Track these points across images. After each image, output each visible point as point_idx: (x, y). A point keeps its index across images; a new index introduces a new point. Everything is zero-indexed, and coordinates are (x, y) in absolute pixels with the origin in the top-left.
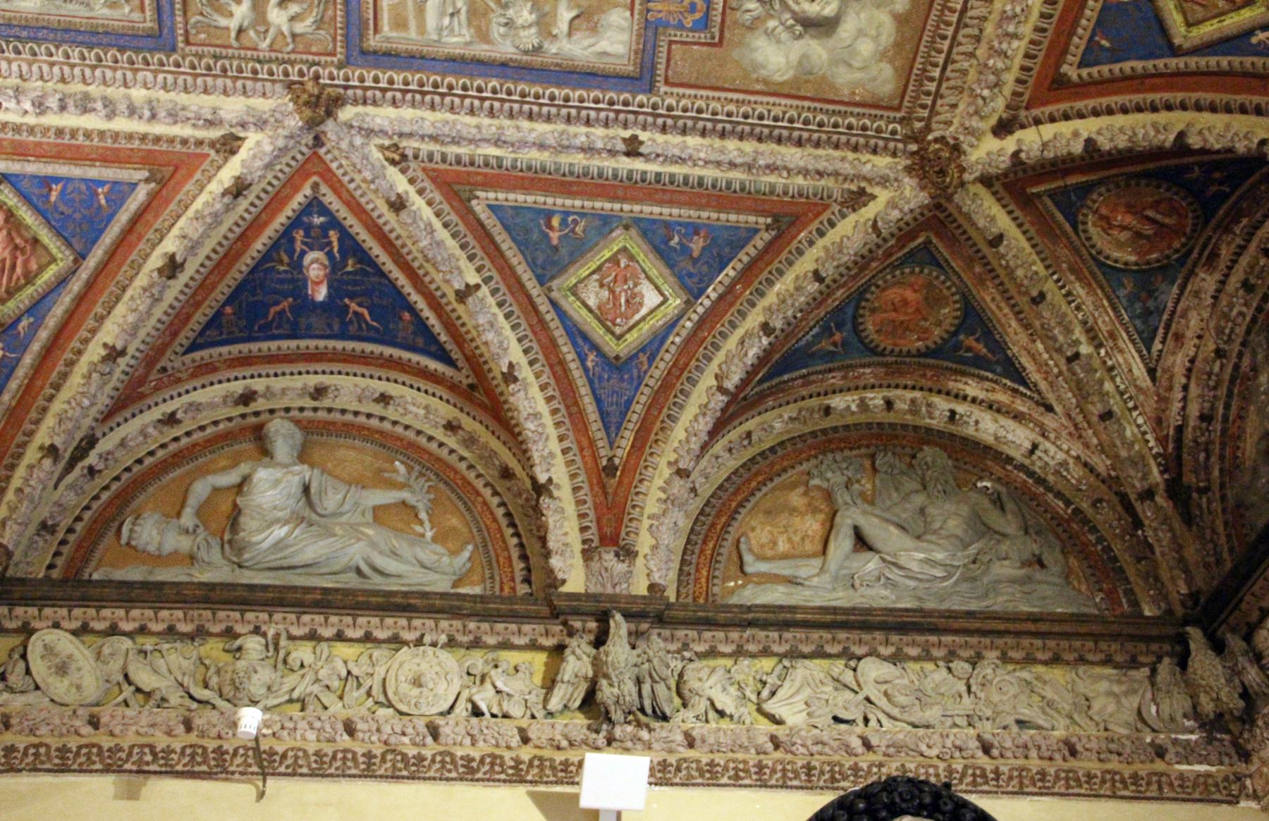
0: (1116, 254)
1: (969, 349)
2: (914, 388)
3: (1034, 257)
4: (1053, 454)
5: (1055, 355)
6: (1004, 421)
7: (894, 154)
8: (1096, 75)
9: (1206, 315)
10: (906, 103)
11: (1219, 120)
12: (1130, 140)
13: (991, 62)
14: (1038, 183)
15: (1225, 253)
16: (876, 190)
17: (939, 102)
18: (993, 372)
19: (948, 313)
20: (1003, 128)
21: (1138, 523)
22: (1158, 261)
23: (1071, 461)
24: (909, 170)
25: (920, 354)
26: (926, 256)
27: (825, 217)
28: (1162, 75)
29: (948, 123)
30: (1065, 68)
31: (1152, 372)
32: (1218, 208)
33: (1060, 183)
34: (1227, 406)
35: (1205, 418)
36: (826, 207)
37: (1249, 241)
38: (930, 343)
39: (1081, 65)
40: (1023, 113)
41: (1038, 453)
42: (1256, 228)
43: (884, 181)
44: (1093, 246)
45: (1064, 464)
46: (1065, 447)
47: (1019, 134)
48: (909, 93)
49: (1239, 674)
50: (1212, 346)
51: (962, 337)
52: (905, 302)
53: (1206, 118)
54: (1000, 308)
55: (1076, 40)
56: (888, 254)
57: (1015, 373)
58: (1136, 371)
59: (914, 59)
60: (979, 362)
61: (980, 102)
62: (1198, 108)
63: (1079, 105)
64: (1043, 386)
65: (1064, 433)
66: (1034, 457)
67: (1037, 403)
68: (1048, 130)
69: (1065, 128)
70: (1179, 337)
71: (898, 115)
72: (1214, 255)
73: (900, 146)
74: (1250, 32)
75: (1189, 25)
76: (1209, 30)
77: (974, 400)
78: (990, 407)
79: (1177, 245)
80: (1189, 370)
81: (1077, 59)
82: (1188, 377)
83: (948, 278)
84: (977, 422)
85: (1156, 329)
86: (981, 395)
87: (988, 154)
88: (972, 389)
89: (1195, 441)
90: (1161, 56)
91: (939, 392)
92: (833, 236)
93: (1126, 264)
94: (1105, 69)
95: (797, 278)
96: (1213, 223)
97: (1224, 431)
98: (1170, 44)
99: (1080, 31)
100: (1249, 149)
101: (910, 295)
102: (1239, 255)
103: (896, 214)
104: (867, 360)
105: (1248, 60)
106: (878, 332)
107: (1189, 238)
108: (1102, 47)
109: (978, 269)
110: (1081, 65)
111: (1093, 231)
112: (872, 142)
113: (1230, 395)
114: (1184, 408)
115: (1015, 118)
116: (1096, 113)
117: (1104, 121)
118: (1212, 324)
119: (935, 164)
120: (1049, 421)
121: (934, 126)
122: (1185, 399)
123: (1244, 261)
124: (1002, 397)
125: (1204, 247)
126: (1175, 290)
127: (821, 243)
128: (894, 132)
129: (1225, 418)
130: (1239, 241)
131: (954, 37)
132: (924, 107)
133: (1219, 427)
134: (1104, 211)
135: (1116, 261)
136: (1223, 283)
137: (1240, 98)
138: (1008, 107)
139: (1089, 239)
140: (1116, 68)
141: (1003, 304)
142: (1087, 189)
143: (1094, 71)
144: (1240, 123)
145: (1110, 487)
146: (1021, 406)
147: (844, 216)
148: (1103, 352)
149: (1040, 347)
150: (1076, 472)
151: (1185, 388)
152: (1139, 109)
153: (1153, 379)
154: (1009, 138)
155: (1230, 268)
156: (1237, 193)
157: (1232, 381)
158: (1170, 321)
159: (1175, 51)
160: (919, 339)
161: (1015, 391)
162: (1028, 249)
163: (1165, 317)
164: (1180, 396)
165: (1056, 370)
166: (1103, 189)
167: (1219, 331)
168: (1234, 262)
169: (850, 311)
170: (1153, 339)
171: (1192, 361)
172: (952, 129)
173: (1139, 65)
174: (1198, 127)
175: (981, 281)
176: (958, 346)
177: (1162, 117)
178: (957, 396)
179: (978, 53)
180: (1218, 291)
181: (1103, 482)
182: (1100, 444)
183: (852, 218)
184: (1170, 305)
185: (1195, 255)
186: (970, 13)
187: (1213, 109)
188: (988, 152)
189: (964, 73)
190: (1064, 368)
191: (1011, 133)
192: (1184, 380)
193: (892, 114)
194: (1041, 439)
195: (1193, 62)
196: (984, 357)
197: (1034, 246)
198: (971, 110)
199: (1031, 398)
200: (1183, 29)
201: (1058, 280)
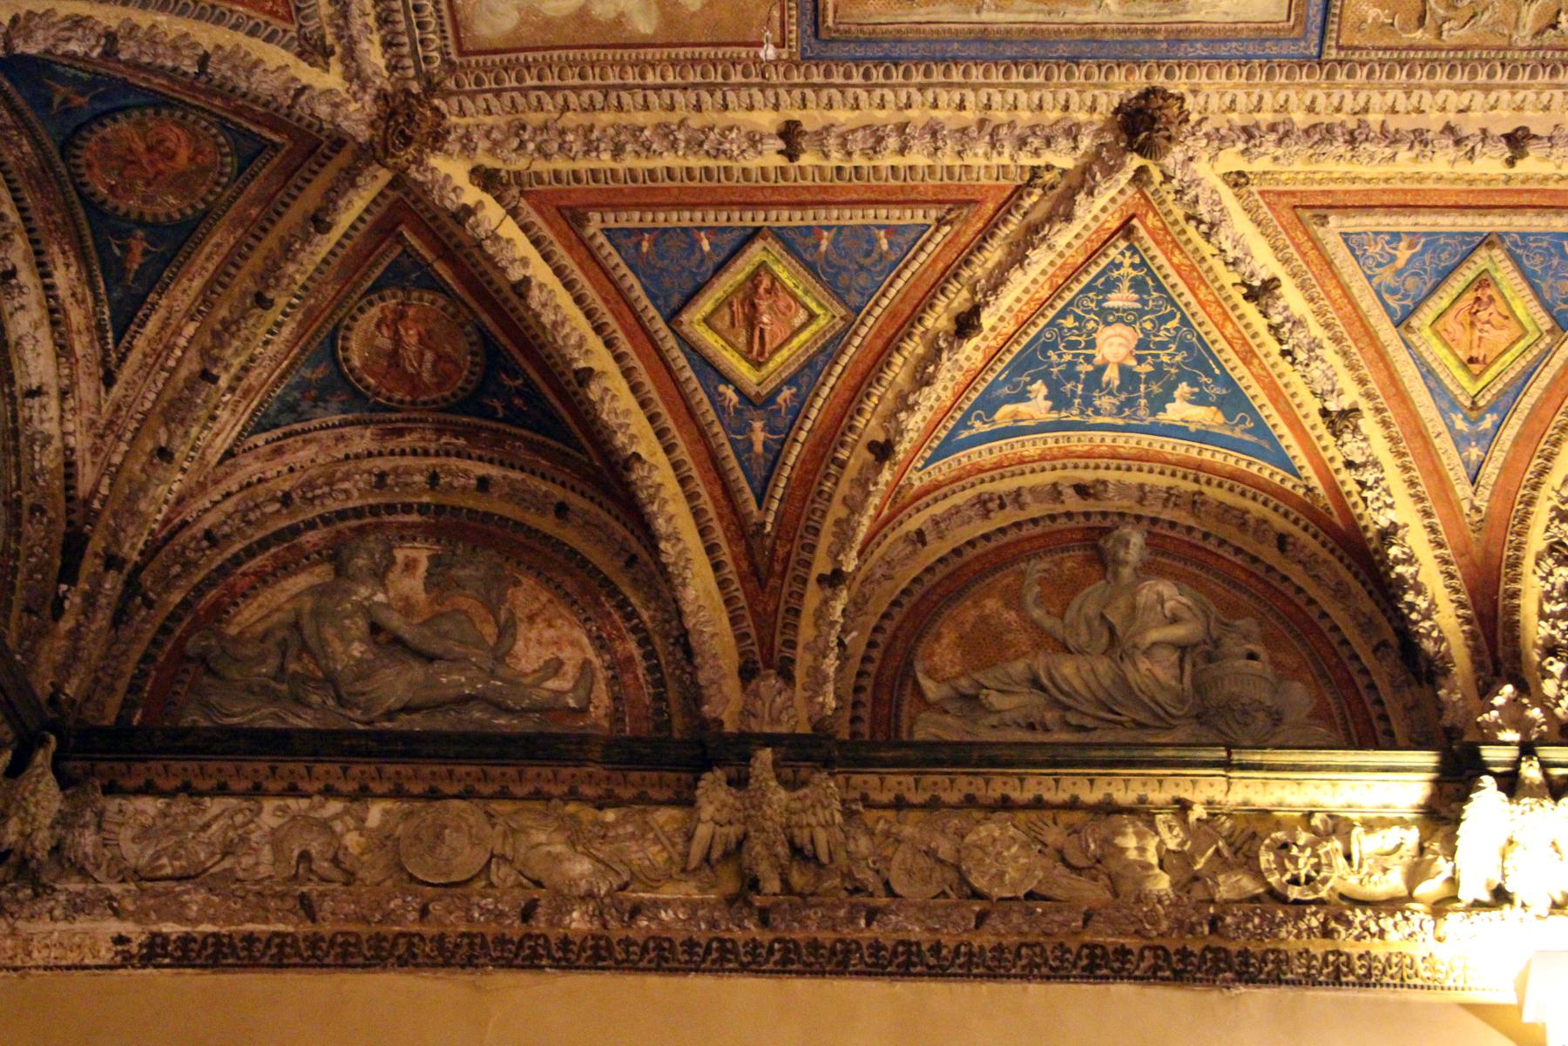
0: (353, 345)
1: (126, 249)
2: (21, 210)
3: (311, 268)
4: (46, 417)
5: (193, 353)
6: (44, 333)
7: (392, 68)
8: (605, 252)
9: (320, 461)
10: (473, 60)
11: (627, 401)
12: (555, 324)
13: (570, 137)
14: (416, 233)
15: (408, 440)
16: (336, 67)
17: (489, 96)
18: (109, 290)
19: (170, 204)
20: (486, 179)
21: (69, 573)
22: (367, 388)
23: (57, 443)
24: (382, 96)
25: (88, 201)
26: (250, 152)
27: (277, 24)
28: (638, 319)
29: (462, 113)
30: (595, 217)
31: (229, 454)
32: (468, 414)
33: (429, 257)
34: (250, 552)
35: (208, 535)
36: (288, 18)
37: (437, 454)
38: (112, 202)
39: (608, 232)
40: (515, 191)
41: (36, 402)
42: (458, 455)
43: (355, 74)
44: (354, 319)
45: (48, 440)
46: (70, 427)
47: (488, 199)
48: (489, 59)
49: (68, 826)
50: (286, 487)
51: (140, 233)
52: (171, 156)
53: (620, 386)
54: (208, 259)
55: (636, 215)
56: (238, 111)
57: (126, 316)
58: (219, 440)
59: (537, 49)
60: (113, 270)
61: (515, 143)
62: (627, 373)
63: (558, 249)
64: (134, 358)
65: (86, 414)
66: (30, 402)
67: (104, 362)
68: (510, 229)
69: (523, 246)
70: (279, 451)
71: (454, 57)
72: (400, 433)
73: (411, 72)
74: (727, 380)
75: (706, 320)
76: (711, 341)
77: (49, 288)
78: (52, 311)
79: (398, 396)
80: (249, 485)
81: (611, 224)
82: (241, 489)
83: (225, 187)
84: (22, 307)
85: (277, 426)
86: (63, 291)
87: (448, 177)
88: (64, 277)
89: (184, 548)
90: (658, 308)
91: (33, 242)
92: (256, 47)
93: (347, 360)
94: (616, 259)
95: (186, 35)
96: (442, 416)
97: (223, 571)
98: (678, 311)
99: (649, 216)
100: (624, 448)
101: (183, 155)
102: (414, 453)
103: (323, 110)
104: (49, 144)
105: (701, 395)
106: (104, 139)
107: (413, 403)
108: (639, 244)
109: (254, 212)
110: (608, 232)
111: (374, 312)
112: (405, 39)
113: (264, 545)
114: (206, 510)
115: (507, 185)
116: (558, 271)
117: (554, 283)
118: (313, 472)
119: (406, 121)
120: (87, 389)
121: (454, 101)
122: (215, 503)
123: (408, 461)
124: (77, 316)
125: (408, 420)
126: (336, 419)
127: (240, 37)
128: (427, 59)
129: (237, 560)
130: (433, 447)
131: (586, 87)
132: (479, 81)
133: (218, 561)
134: (411, 312)
135: (345, 349)
136: (370, 455)
137: (661, 408)
138: (518, 174)
139: (361, 310)
140: (624, 269)
141: (217, 259)
142: (433, 284)
143: (608, 248)
144: (638, 423)
145: (69, 511)
146: (81, 344)
147: (286, 47)
148: (228, 397)
149: (190, 329)
150: (49, 459)
151: (228, 495)
152: (589, 314)
153: (220, 462)
154: (477, 190)
155: (392, 453)
156: (501, 426)
157: (279, 536)
158: (297, 433)
159: (672, 318)
160: (112, 189)
161: (100, 327)
162: (318, 259)
163: (297, 427)
164: (217, 497)
165: (172, 363)
166: (441, 302)
167: (310, 484)
168: (403, 453)
169: (131, 100)
170: (265, 430)
171: (260, 480)
172: (454, 119)
173: (638, 291)
174: (608, 384)
175: (240, 221)
176: (123, 234)
177: (595, 342)
178: (40, 264)
179: (569, 114)
180: (357, 456)
181: (69, 499)
182: (120, 467)
183: (288, 58)
184: (315, 423)
185: (394, 416)
186: (624, 94)
187: (635, 388)
188: (450, 172)
189: (540, 107)
190: (183, 373)
191: (485, 189)
192: (234, 488)
193: (452, 49)
194: (54, 392)
195: (670, 343)
196: (124, 271)
197: (325, 261)
198: (495, 135)
199: (106, 353)
200: (699, 316)
201: (291, 305)
